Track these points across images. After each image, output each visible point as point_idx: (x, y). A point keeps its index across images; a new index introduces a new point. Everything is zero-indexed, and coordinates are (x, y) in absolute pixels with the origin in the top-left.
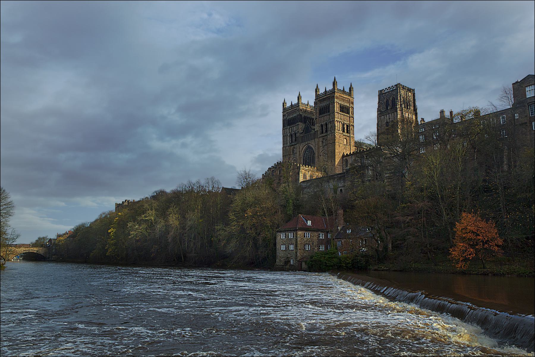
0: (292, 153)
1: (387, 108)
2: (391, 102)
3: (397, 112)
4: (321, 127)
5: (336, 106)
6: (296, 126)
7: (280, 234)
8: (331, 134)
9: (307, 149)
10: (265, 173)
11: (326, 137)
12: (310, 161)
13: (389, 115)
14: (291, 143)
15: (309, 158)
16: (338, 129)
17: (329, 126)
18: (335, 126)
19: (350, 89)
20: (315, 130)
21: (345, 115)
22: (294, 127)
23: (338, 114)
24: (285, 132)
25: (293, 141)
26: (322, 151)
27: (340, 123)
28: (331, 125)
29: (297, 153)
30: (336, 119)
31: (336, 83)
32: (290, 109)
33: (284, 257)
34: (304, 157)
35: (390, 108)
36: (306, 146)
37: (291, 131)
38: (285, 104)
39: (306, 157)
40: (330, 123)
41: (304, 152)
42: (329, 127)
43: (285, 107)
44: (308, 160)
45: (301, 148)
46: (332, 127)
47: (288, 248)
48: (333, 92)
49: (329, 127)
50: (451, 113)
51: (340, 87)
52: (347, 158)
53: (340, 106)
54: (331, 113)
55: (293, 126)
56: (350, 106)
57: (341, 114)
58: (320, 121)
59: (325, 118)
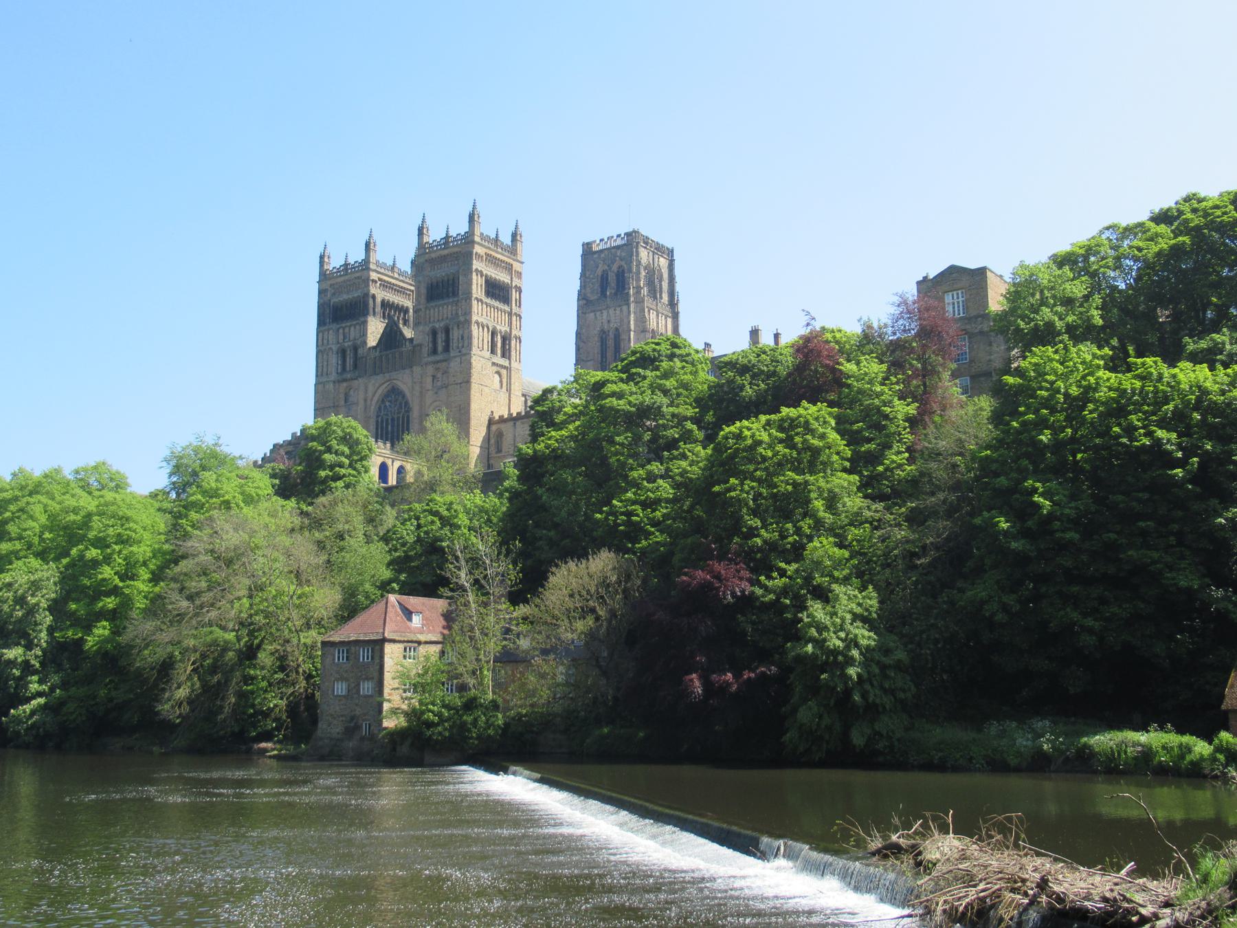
0: (342, 403)
1: (603, 293)
2: (615, 278)
3: (628, 305)
4: (431, 336)
5: (474, 281)
6: (358, 327)
7: (332, 649)
8: (458, 360)
9: (386, 396)
10: (263, 459)
11: (444, 364)
12: (395, 430)
13: (608, 312)
14: (341, 374)
15: (393, 420)
16: (480, 346)
17: (455, 334)
18: (470, 337)
19: (514, 236)
20: (414, 342)
21: (497, 308)
22: (352, 328)
23: (480, 303)
24: (325, 342)
25: (348, 369)
26: (434, 402)
27: (486, 329)
28: (461, 332)
29: (357, 404)
30: (474, 318)
31: (476, 217)
32: (341, 276)
33: (342, 716)
34: (378, 417)
35: (611, 293)
36: (386, 385)
37: (341, 337)
38: (326, 260)
39: (385, 417)
40: (458, 328)
41: (377, 402)
42: (456, 338)
43: (325, 268)
44: (390, 427)
45: (371, 389)
46: (462, 338)
47: (354, 691)
48: (468, 239)
49: (456, 338)
50: (777, 336)
51: (485, 227)
52: (503, 426)
53: (486, 281)
54: (462, 299)
55: (348, 324)
56: (514, 285)
57: (486, 304)
58: (428, 317)
59: (443, 311)
